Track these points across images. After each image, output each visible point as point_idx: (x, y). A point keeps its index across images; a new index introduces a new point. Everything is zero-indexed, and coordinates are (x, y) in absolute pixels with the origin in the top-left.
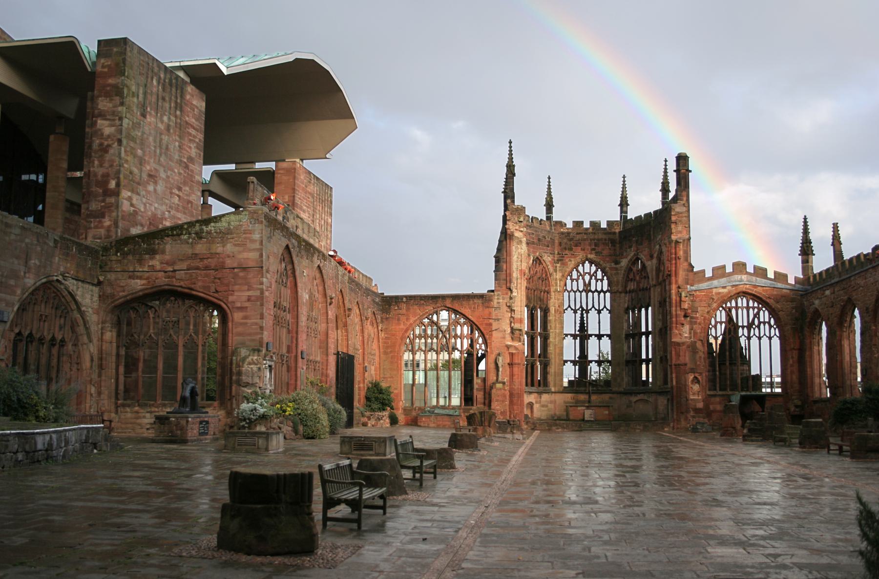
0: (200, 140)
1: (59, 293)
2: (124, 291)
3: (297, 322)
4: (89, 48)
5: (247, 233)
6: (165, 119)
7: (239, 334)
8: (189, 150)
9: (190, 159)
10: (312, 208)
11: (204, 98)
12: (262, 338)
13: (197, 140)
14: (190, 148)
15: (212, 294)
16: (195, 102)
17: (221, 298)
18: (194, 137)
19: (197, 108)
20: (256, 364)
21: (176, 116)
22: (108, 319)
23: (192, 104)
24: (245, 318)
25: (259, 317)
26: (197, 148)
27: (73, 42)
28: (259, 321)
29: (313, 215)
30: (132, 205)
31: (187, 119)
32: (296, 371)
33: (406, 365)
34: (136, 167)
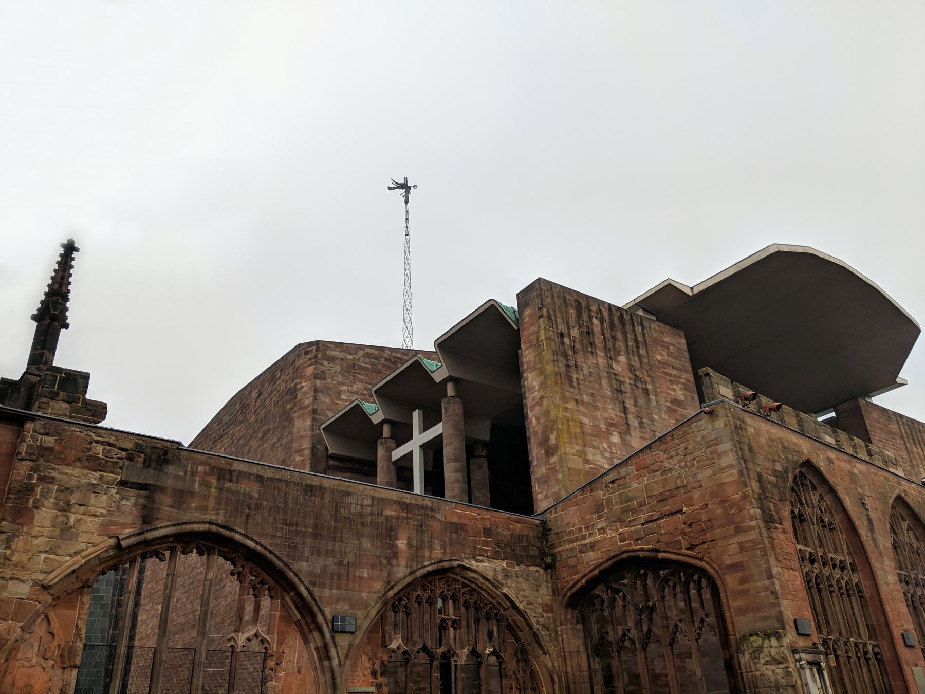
0: (687, 381)
1: (473, 586)
2: (577, 573)
3: (876, 584)
4: (509, 302)
5: (712, 446)
6: (622, 359)
7: (743, 611)
8: (672, 393)
9: (676, 402)
10: (905, 451)
11: (683, 334)
12: (780, 612)
13: (683, 381)
14: (674, 390)
15: (684, 551)
16: (666, 340)
17: (700, 556)
18: (676, 376)
19: (673, 345)
20: (780, 663)
21: (640, 356)
22: (569, 617)
23: (663, 341)
24: (744, 580)
25: (765, 576)
26: (686, 389)
27: (492, 305)
28: (767, 582)
29: (911, 461)
30: (587, 461)
31: (659, 358)
32: (901, 671)
33: (574, 349)
34: (584, 414)
